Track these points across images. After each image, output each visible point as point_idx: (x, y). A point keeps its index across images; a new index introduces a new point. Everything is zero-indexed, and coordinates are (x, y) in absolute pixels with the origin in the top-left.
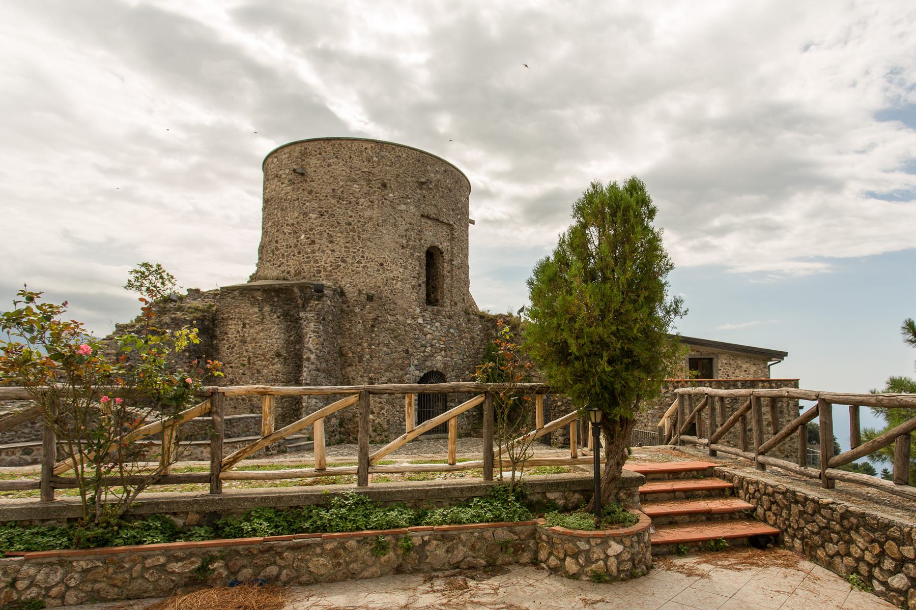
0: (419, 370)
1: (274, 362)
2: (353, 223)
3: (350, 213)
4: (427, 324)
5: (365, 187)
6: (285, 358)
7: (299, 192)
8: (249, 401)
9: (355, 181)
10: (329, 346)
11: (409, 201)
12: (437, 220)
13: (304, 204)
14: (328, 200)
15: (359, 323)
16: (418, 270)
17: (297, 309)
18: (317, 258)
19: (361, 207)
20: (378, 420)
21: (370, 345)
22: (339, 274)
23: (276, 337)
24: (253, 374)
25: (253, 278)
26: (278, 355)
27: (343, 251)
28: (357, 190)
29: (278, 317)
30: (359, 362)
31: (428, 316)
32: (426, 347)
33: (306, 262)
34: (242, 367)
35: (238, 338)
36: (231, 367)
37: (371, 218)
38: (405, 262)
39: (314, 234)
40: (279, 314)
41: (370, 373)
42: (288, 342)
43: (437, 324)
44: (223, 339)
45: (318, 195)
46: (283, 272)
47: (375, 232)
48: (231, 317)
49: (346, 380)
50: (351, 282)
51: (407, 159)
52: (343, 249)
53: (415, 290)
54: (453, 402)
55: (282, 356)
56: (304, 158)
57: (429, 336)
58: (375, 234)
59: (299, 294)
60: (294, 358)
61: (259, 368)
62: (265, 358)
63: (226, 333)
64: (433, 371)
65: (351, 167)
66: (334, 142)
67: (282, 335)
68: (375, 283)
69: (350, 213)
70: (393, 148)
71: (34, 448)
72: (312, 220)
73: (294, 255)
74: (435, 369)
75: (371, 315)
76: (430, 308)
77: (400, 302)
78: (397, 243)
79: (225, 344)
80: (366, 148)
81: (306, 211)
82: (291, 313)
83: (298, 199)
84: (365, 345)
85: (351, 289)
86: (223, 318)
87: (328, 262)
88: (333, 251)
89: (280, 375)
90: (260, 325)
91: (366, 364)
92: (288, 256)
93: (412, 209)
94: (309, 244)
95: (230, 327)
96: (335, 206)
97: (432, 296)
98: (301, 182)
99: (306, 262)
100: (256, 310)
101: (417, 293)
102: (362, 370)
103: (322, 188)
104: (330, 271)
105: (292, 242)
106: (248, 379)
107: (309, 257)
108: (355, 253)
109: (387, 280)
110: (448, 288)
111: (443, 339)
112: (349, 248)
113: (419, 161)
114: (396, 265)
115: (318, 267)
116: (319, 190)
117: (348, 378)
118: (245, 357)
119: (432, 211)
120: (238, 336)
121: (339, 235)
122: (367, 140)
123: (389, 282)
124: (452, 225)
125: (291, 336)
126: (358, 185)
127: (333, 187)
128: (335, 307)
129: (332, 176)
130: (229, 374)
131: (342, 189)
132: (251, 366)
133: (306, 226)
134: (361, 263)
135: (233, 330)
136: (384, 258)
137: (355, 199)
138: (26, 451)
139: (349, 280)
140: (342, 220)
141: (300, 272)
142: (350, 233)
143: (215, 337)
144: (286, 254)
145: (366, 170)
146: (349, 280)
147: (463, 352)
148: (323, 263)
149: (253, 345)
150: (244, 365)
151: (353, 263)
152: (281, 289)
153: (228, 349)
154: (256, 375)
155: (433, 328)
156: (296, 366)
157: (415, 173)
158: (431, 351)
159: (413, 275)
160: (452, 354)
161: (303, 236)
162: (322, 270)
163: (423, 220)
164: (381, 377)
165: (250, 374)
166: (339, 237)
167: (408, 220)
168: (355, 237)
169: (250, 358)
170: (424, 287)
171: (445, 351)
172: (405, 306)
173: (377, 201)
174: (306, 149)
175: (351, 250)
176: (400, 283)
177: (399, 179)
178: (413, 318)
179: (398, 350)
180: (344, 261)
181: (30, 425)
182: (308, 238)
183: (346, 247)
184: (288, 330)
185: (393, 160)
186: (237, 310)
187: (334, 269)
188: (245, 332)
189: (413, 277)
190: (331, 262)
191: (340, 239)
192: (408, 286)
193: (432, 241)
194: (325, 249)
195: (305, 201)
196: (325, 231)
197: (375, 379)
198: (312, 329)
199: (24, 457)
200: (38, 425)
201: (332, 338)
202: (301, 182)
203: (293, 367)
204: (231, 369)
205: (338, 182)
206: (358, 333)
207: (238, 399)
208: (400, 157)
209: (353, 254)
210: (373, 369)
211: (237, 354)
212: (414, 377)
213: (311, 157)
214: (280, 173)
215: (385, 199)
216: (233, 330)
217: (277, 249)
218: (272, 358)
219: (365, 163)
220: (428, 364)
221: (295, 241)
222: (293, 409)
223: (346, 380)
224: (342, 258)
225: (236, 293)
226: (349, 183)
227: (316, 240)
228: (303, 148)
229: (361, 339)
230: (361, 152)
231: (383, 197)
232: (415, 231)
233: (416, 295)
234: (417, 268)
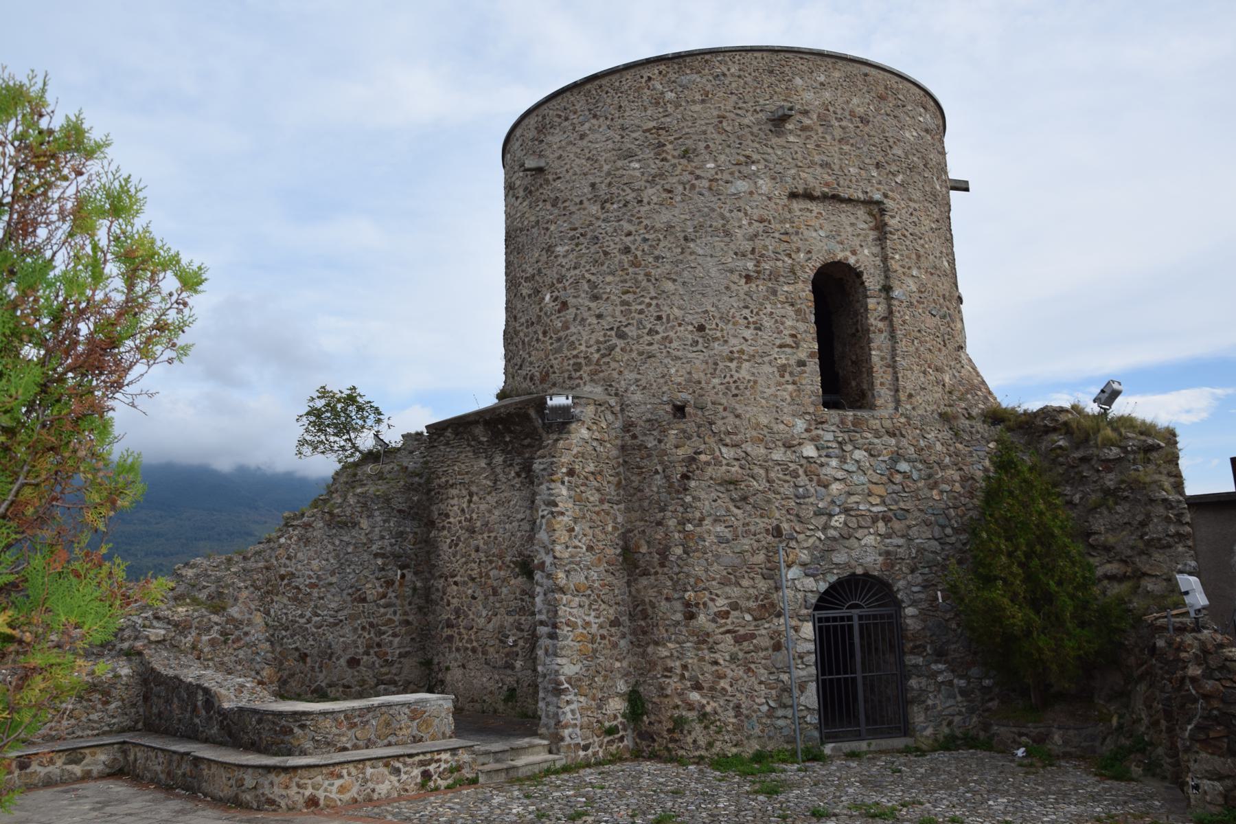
0: (813, 576)
2: (633, 247)
3: (627, 227)
4: (827, 456)
5: (651, 162)
7: (538, 209)
9: (630, 155)
10: (590, 532)
11: (754, 168)
12: (836, 198)
14: (584, 209)
15: (657, 472)
16: (793, 327)
18: (573, 339)
19: (647, 208)
20: (712, 703)
21: (682, 523)
22: (613, 365)
25: (501, 396)
27: (618, 313)
28: (637, 174)
29: (518, 475)
30: (662, 565)
31: (830, 436)
32: (831, 516)
34: (470, 584)
35: (464, 523)
36: (456, 583)
37: (669, 228)
38: (757, 314)
41: (686, 591)
43: (859, 454)
44: (444, 528)
45: (566, 204)
47: (680, 257)
48: (451, 482)
49: (640, 608)
50: (638, 381)
51: (739, 77)
53: (787, 377)
54: (919, 654)
57: (835, 487)
58: (681, 262)
61: (495, 584)
63: (447, 516)
64: (854, 574)
65: (623, 128)
66: (588, 86)
68: (690, 373)
69: (627, 227)
70: (706, 61)
71: (87, 751)
72: (560, 260)
73: (538, 340)
74: (859, 571)
75: (680, 452)
76: (833, 415)
77: (749, 412)
78: (732, 271)
79: (445, 537)
80: (650, 79)
84: (672, 523)
85: (638, 397)
86: (439, 485)
88: (599, 316)
90: (494, 494)
91: (676, 569)
93: (765, 185)
94: (559, 311)
96: (598, 219)
97: (854, 384)
98: (541, 185)
100: (483, 463)
101: (794, 383)
102: (669, 583)
108: (641, 312)
109: (716, 364)
110: (882, 359)
111: (880, 490)
112: (628, 304)
113: (771, 72)
114: (735, 324)
115: (576, 356)
117: (643, 602)
119: (815, 179)
121: (609, 278)
123: (721, 365)
124: (878, 203)
127: (591, 179)
128: (601, 442)
129: (588, 159)
130: (453, 597)
131: (609, 179)
132: (483, 580)
133: (552, 274)
134: (657, 333)
135: (455, 503)
136: (707, 312)
137: (634, 195)
138: (72, 757)
139: (633, 376)
140: (613, 246)
141: (547, 374)
142: (631, 270)
143: (431, 524)
144: (526, 340)
145: (651, 124)
146: (633, 376)
147: (942, 520)
148: (583, 348)
149: (485, 535)
150: (473, 579)
151: (639, 337)
153: (450, 548)
154: (491, 599)
155: (846, 467)
157: (762, 102)
158: (846, 524)
159: (778, 342)
160: (909, 527)
161: (548, 297)
163: (796, 205)
164: (713, 600)
166: (609, 284)
167: (756, 214)
168: (640, 278)
170: (814, 366)
171: (887, 520)
172: (764, 420)
173: (680, 188)
174: (544, 118)
175: (633, 308)
176: (746, 365)
177: (725, 124)
178: (788, 446)
179: (752, 528)
180: (622, 335)
181: (100, 706)
183: (624, 303)
185: (709, 87)
187: (603, 356)
189: (781, 346)
190: (598, 342)
191: (611, 286)
192: (767, 369)
193: (829, 252)
194: (586, 315)
196: (583, 277)
197: (697, 605)
199: (69, 767)
200: (113, 706)
201: (598, 513)
204: (455, 588)
205: (601, 167)
206: (656, 497)
207: (467, 649)
208: (724, 75)
209: (637, 316)
210: (692, 581)
211: (463, 556)
212: (800, 596)
215: (698, 177)
216: (456, 508)
219: (649, 113)
220: (840, 557)
223: (640, 608)
224: (618, 328)
225: (448, 433)
226: (620, 163)
227: (571, 301)
228: (540, 118)
229: (662, 510)
230: (638, 90)
231: (692, 173)
232: (777, 235)
233: (790, 387)
234: (789, 323)
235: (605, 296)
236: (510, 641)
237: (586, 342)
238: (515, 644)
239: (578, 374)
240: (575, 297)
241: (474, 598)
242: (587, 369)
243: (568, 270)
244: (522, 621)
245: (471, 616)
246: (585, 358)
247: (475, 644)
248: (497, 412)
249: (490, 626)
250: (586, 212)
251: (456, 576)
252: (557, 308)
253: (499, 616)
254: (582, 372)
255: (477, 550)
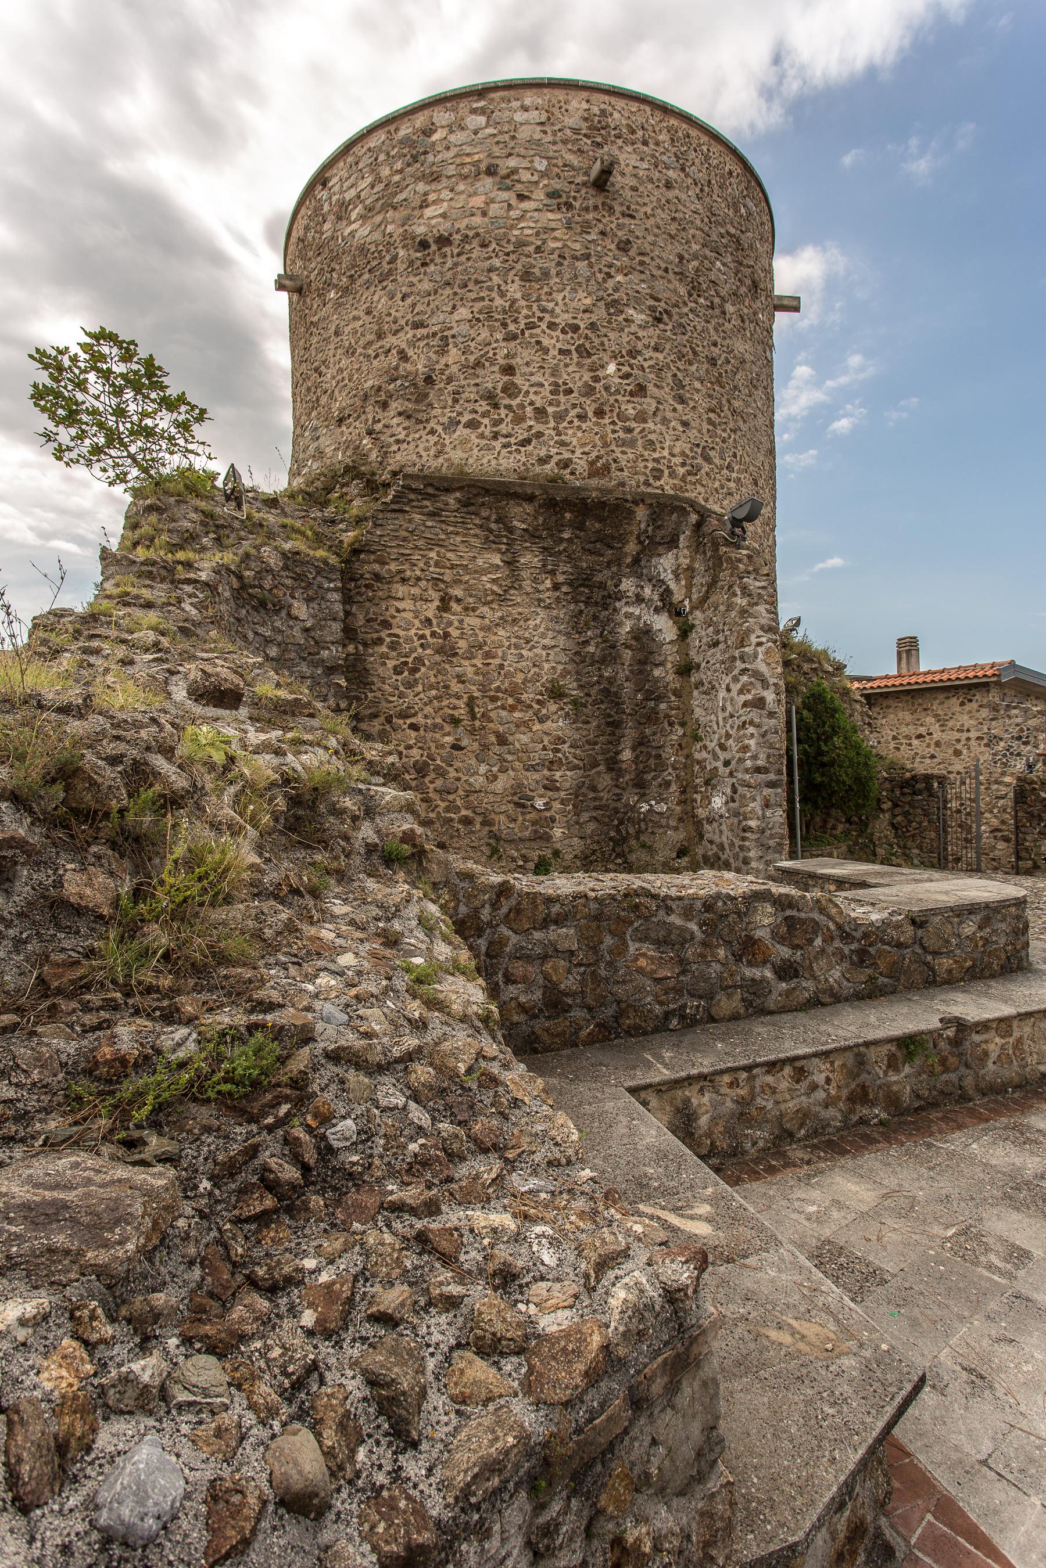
1: (544, 711)
6: (575, 702)
8: (483, 824)
13: (609, 276)
17: (614, 569)
18: (652, 437)
22: (700, 489)
23: (547, 642)
24: (485, 747)
26: (556, 693)
27: (705, 431)
29: (556, 587)
33: (624, 443)
34: (447, 728)
36: (414, 727)
39: (643, 369)
40: (561, 578)
42: (579, 658)
44: (380, 641)
46: (543, 461)
48: (408, 573)
52: (705, 426)
55: (566, 696)
56: (599, 139)
59: (643, 526)
60: (602, 702)
62: (519, 701)
63: (386, 624)
67: (562, 640)
72: (633, 328)
79: (385, 656)
81: (616, 296)
82: (598, 578)
83: (587, 257)
86: (377, 577)
87: (677, 451)
88: (685, 424)
89: (565, 747)
92: (560, 417)
94: (631, 394)
95: (401, 605)
99: (624, 443)
100: (497, 560)
103: (653, 244)
104: (683, 479)
105: (576, 376)
106: (473, 761)
107: (630, 430)
116: (648, 248)
118: (458, 697)
120: (427, 632)
121: (697, 385)
122: (734, 152)
125: (586, 643)
126: (724, 264)
129: (674, 219)
130: (409, 747)
132: (477, 723)
133: (616, 340)
141: (607, 468)
144: (550, 410)
145: (733, 231)
149: (478, 662)
150: (455, 721)
152: (602, 505)
154: (496, 749)
156: (608, 724)
161: (611, 368)
162: (666, 472)
165: (476, 745)
166: (698, 391)
168: (724, 402)
169: (471, 703)
174: (603, 112)
180: (708, 459)
182: (627, 376)
184: (576, 624)
186: (433, 555)
187: (689, 473)
188: (450, 624)
190: (683, 454)
194: (669, 415)
195: (610, 266)
198: (763, 621)
202: (596, 208)
203: (598, 726)
204: (413, 734)
207: (452, 820)
211: (431, 687)
213: (620, 142)
214: (512, 163)
217: (511, 390)
218: (539, 702)
221: (587, 377)
222: (611, 839)
225: (451, 500)
227: (650, 387)
228: (596, 110)
235: (691, 404)
236: (539, 803)
237: (671, 448)
238: (548, 806)
239: (658, 483)
240: (655, 385)
241: (456, 747)
242: (671, 481)
243: (647, 347)
244: (557, 778)
245: (453, 774)
246: (669, 467)
247: (464, 812)
248: (584, 494)
249: (499, 786)
250: (670, 286)
251: (415, 715)
252: (629, 388)
253: (511, 772)
254: (662, 482)
255: (461, 679)
